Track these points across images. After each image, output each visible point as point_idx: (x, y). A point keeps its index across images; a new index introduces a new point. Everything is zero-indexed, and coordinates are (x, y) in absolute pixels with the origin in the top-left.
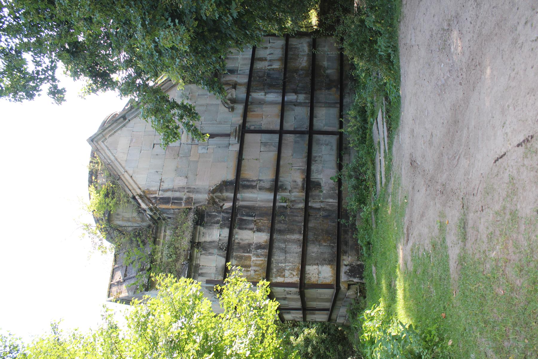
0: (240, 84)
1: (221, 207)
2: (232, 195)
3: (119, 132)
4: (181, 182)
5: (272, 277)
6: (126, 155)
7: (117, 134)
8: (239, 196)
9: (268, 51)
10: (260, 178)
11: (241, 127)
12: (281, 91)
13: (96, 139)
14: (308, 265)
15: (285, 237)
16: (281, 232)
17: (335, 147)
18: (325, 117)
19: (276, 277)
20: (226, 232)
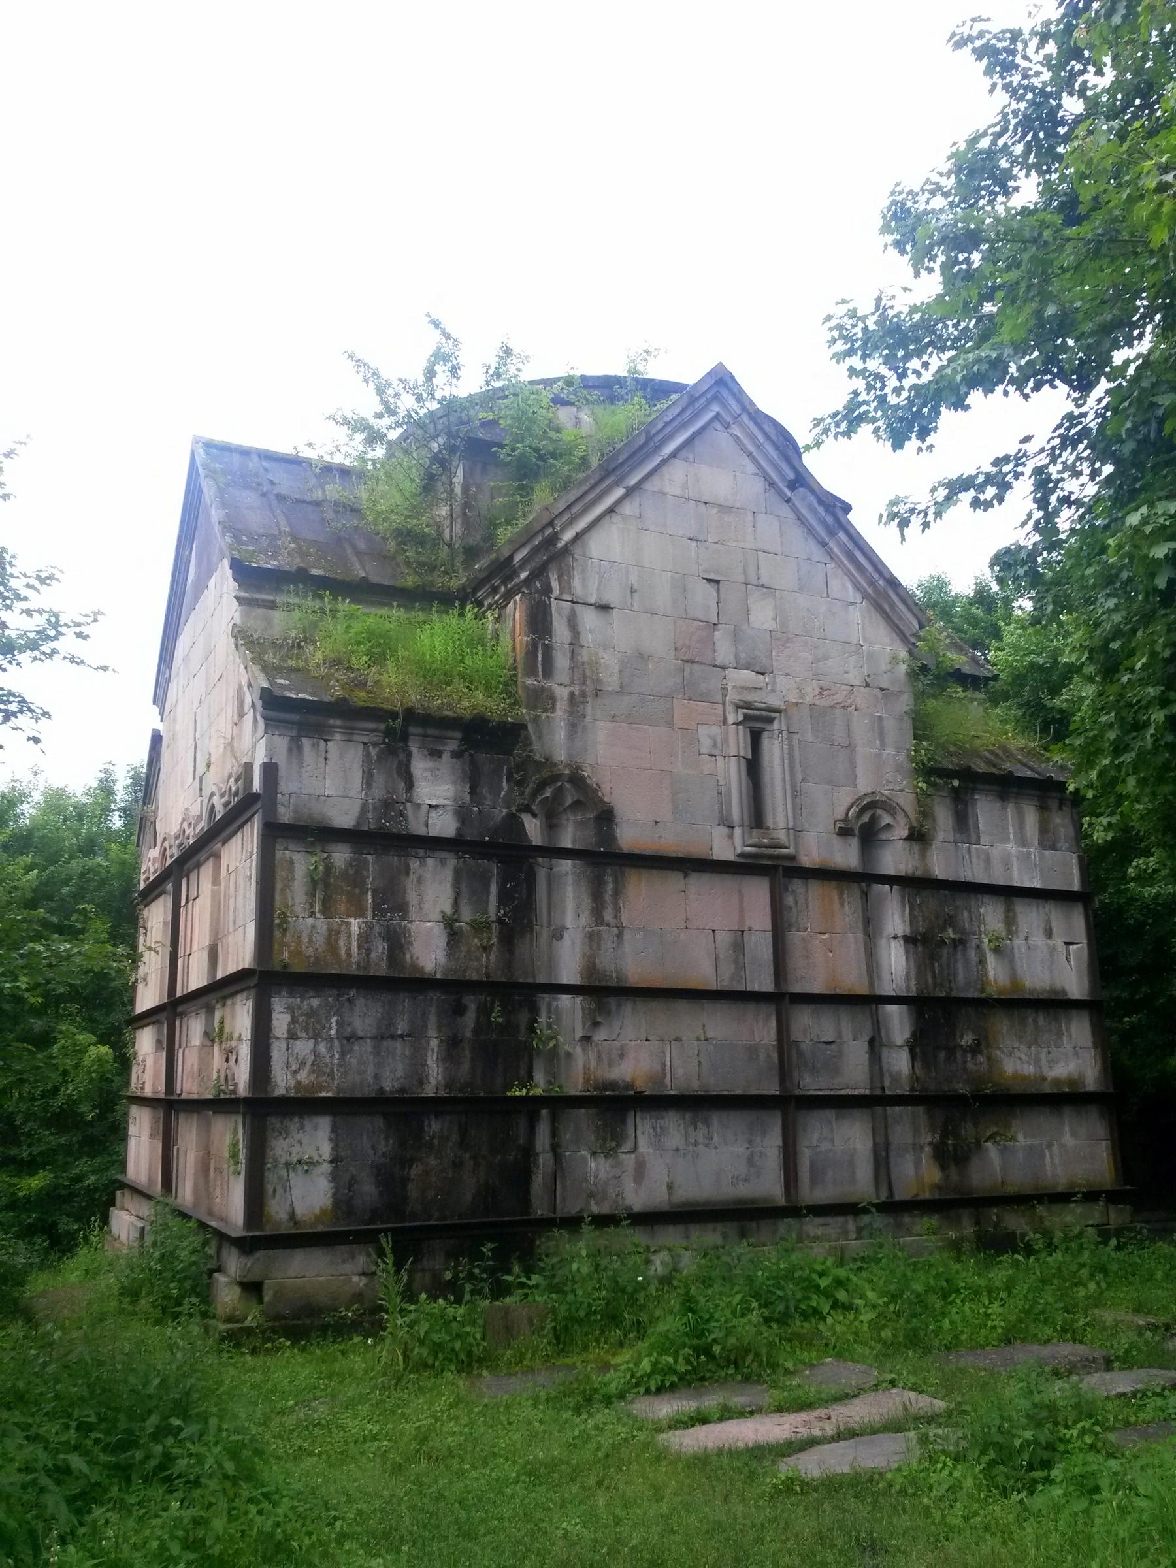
0: (923, 855)
1: (527, 809)
2: (567, 843)
3: (751, 467)
5: (291, 994)
6: (678, 493)
7: (746, 461)
8: (566, 866)
9: (1038, 940)
10: (627, 936)
11: (787, 864)
12: (913, 992)
13: (725, 393)
14: (334, 1129)
15: (432, 1032)
17: (745, 1191)
18: (844, 1150)
19: (290, 1009)
20: (443, 825)
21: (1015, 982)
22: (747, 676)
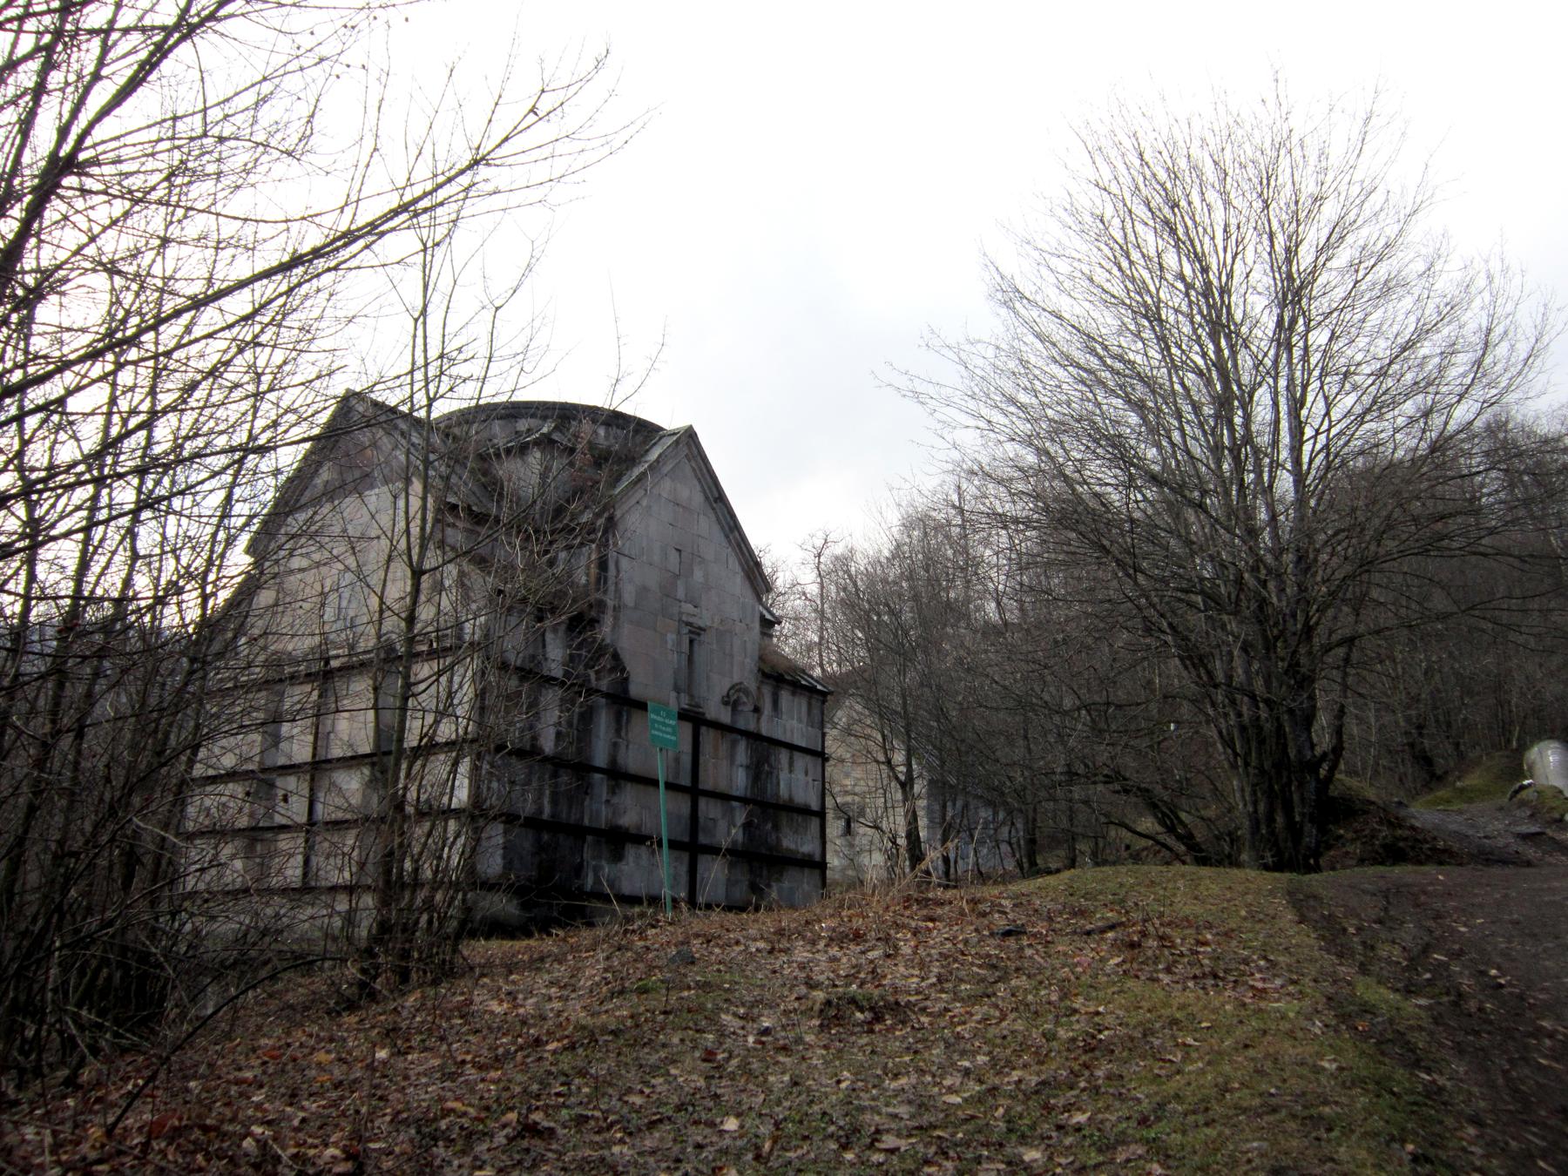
2: (604, 689)
4: (629, 596)
9: (801, 776)
16: (555, 775)
21: (791, 799)
22: (688, 607)
